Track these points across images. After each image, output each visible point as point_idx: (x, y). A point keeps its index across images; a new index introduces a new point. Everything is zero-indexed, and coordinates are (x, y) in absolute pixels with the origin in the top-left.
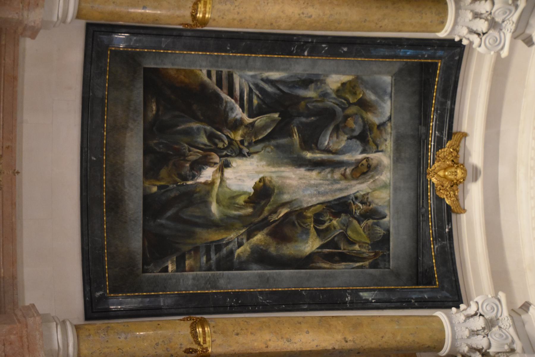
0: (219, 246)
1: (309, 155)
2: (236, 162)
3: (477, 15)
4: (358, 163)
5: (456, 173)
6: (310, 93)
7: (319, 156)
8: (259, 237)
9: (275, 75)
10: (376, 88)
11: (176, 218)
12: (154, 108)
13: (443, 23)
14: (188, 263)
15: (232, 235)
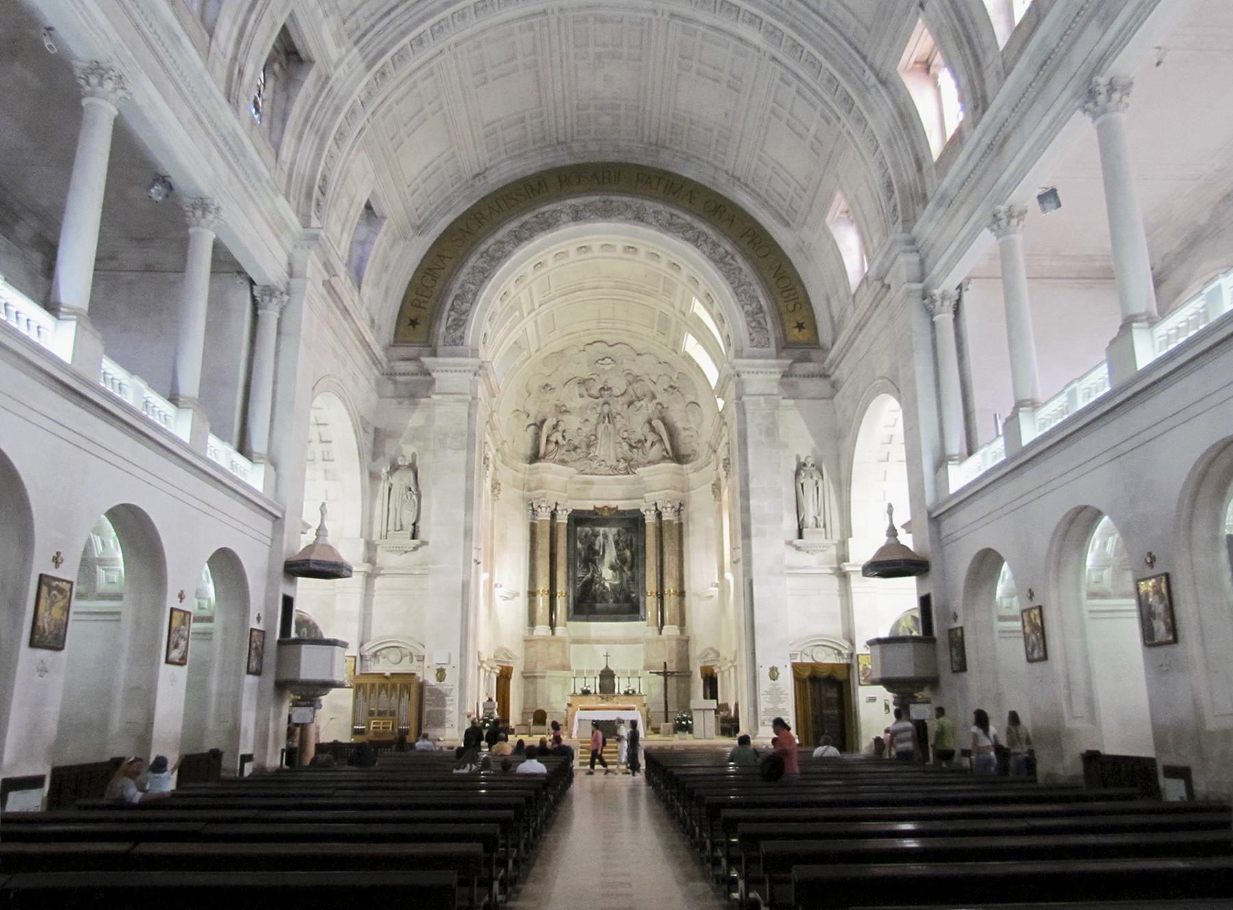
0: (627, 581)
1: (601, 553)
2: (603, 576)
3: (562, 514)
4: (604, 538)
5: (607, 537)
6: (583, 553)
7: (601, 550)
8: (625, 569)
9: (578, 564)
10: (581, 532)
11: (620, 594)
12: (588, 601)
13: (564, 523)
14: (632, 590)
15: (625, 576)
